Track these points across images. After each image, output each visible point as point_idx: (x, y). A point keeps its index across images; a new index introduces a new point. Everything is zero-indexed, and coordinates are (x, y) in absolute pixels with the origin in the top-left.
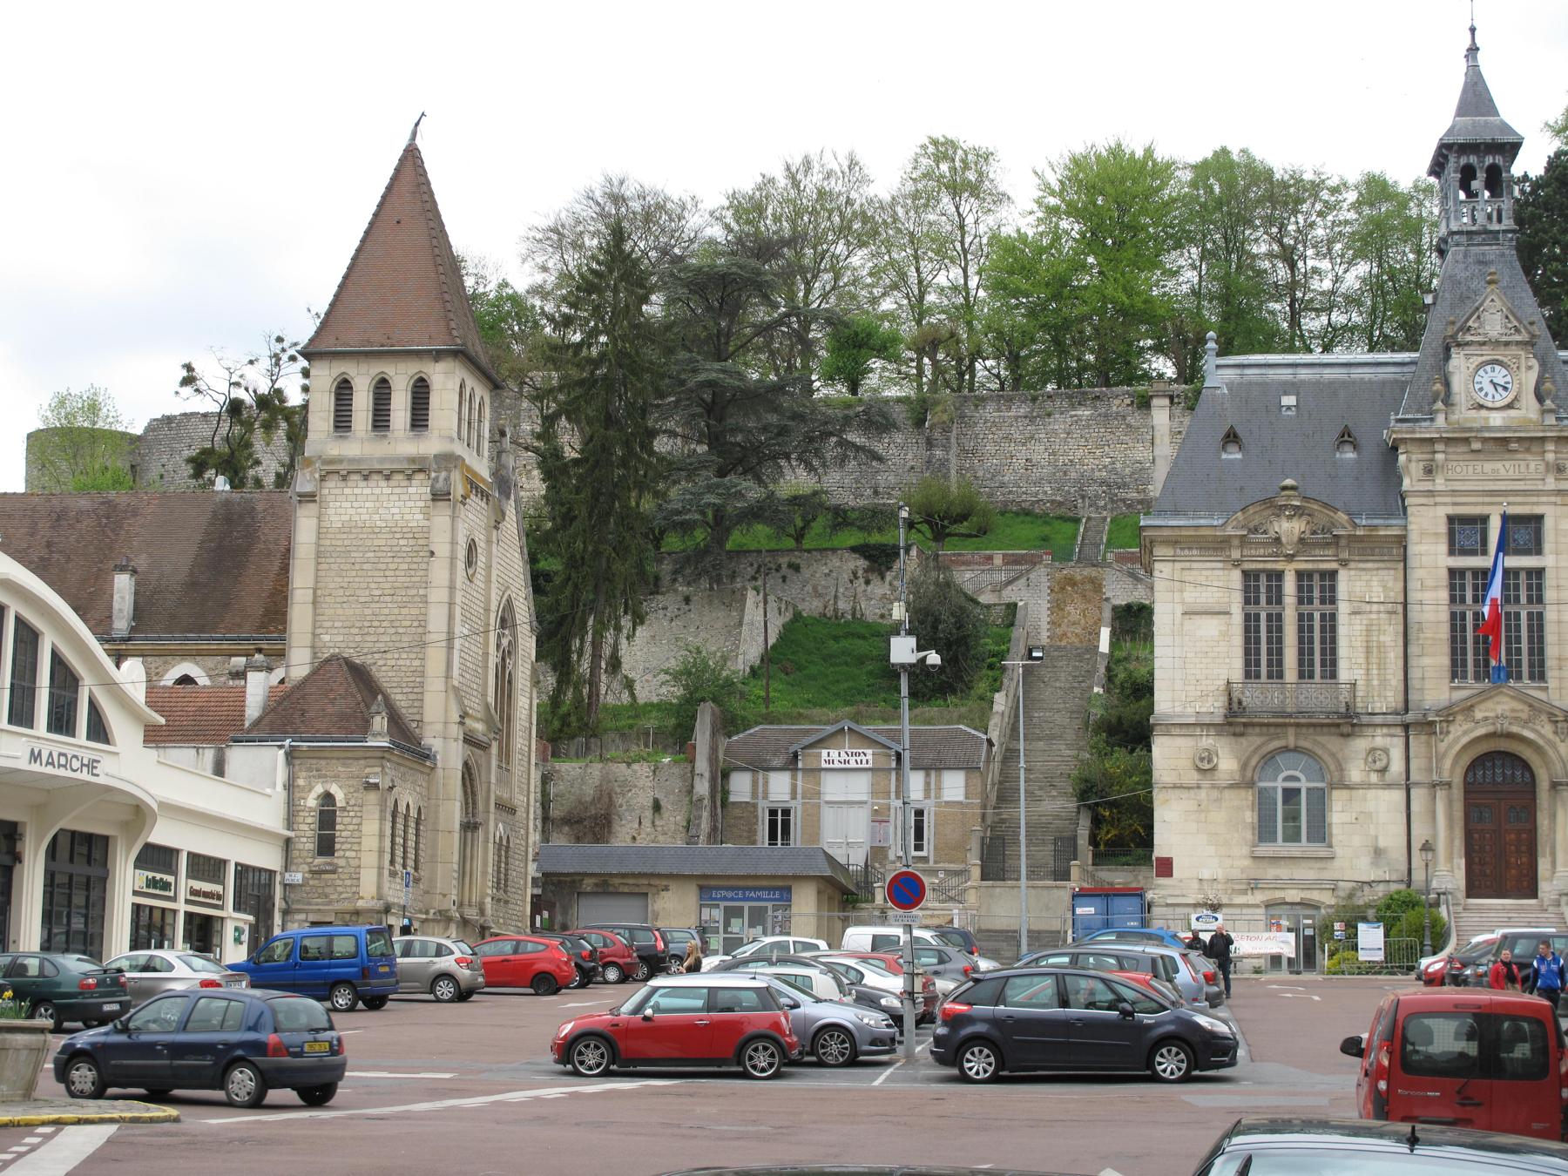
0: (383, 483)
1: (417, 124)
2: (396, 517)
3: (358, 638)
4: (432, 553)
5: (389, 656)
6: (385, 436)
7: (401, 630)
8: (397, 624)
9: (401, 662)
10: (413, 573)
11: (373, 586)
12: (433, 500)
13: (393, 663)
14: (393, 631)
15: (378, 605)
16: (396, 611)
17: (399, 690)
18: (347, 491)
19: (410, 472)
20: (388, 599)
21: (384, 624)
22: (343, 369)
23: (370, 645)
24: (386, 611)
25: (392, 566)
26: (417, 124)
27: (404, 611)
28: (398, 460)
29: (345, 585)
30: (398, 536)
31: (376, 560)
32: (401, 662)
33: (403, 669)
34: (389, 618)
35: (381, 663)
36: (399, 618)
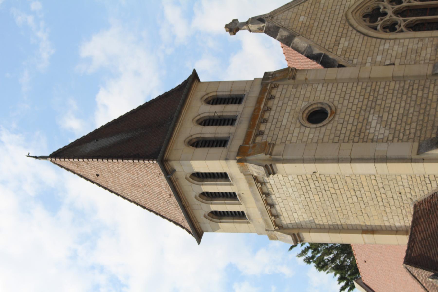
0: (273, 197)
1: (36, 157)
2: (295, 189)
3: (393, 208)
4: (314, 172)
5: (403, 191)
6: (239, 195)
7: (380, 185)
8: (376, 188)
9: (406, 184)
10: (333, 180)
11: (350, 201)
12: (274, 173)
13: (408, 190)
14: (382, 190)
15: (365, 198)
16: (366, 188)
17: (429, 186)
18: (285, 215)
19: (259, 185)
20: (358, 193)
21: (378, 194)
22: (202, 217)
23: (397, 202)
24: (368, 194)
25: (333, 191)
26: (36, 157)
27: (365, 184)
28: (253, 192)
29: (355, 215)
30: (308, 188)
31: (331, 200)
32: (406, 184)
33: (411, 183)
34: (372, 191)
35: (409, 196)
36: (371, 186)
